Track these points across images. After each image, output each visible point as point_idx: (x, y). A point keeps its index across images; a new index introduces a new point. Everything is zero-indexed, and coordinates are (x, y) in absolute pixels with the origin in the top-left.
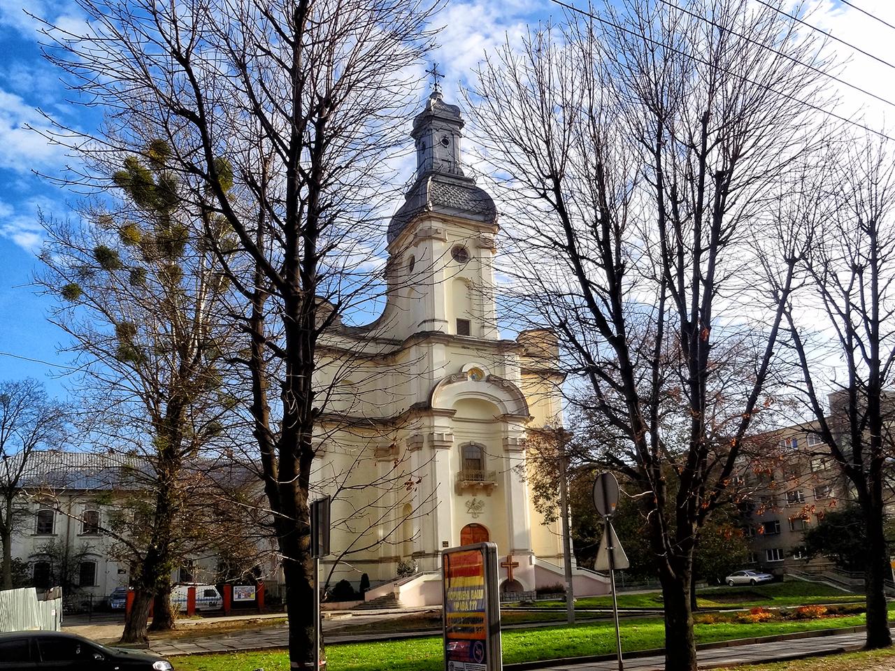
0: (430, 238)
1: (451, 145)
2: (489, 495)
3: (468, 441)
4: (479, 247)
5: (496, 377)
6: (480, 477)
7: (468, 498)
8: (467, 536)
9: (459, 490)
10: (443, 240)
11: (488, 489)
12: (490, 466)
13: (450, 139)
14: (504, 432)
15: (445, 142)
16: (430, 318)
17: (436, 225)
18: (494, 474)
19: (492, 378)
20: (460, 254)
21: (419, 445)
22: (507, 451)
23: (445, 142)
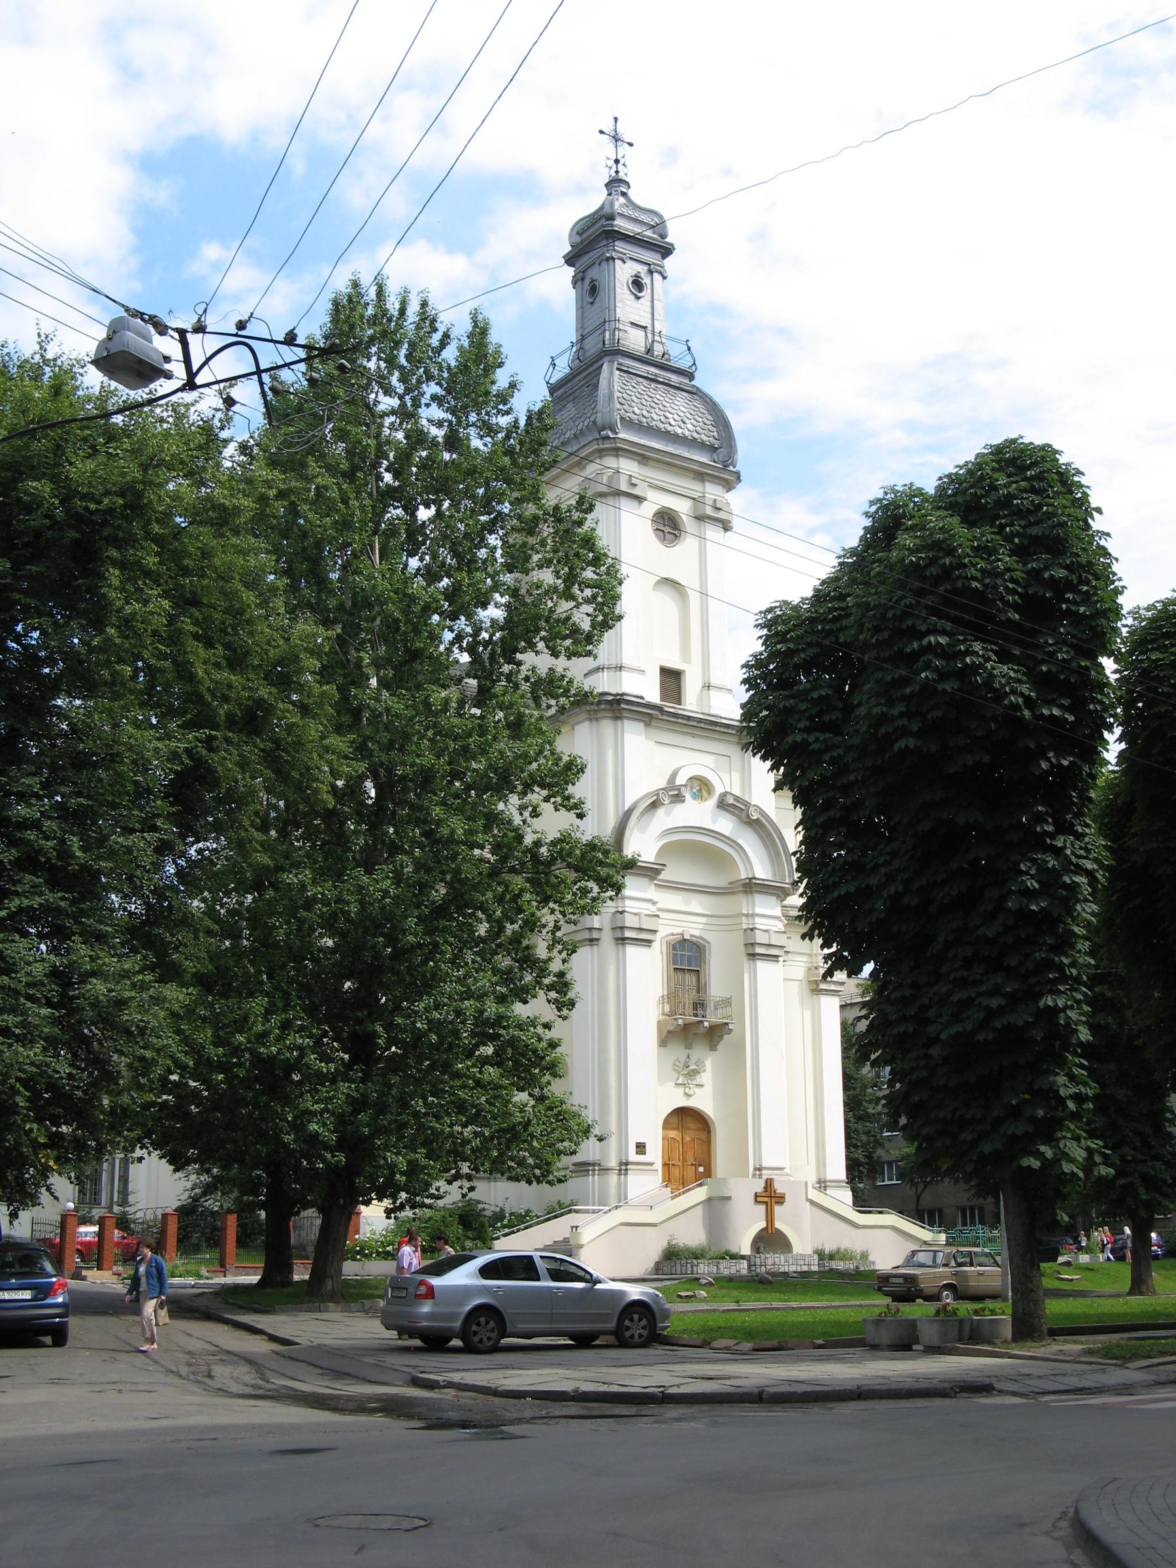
0: (619, 493)
1: (646, 293)
2: (713, 1048)
3: (679, 930)
4: (700, 518)
5: (737, 798)
6: (699, 1005)
7: (677, 1052)
8: (673, 1134)
9: (667, 1037)
10: (639, 499)
11: (714, 1035)
12: (716, 988)
13: (646, 280)
14: (747, 915)
15: (637, 284)
16: (613, 662)
17: (628, 466)
18: (727, 1002)
19: (731, 801)
20: (668, 525)
21: (595, 935)
22: (753, 956)
23: (637, 284)
